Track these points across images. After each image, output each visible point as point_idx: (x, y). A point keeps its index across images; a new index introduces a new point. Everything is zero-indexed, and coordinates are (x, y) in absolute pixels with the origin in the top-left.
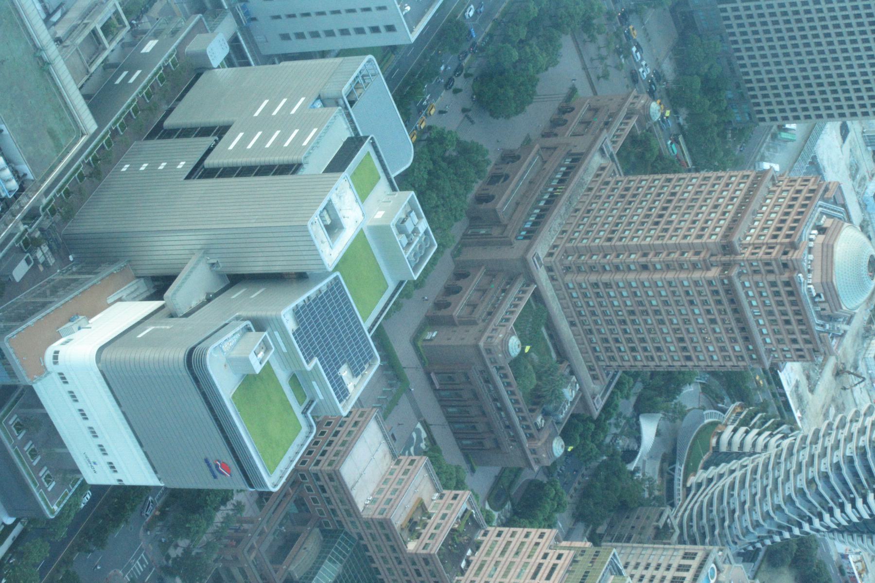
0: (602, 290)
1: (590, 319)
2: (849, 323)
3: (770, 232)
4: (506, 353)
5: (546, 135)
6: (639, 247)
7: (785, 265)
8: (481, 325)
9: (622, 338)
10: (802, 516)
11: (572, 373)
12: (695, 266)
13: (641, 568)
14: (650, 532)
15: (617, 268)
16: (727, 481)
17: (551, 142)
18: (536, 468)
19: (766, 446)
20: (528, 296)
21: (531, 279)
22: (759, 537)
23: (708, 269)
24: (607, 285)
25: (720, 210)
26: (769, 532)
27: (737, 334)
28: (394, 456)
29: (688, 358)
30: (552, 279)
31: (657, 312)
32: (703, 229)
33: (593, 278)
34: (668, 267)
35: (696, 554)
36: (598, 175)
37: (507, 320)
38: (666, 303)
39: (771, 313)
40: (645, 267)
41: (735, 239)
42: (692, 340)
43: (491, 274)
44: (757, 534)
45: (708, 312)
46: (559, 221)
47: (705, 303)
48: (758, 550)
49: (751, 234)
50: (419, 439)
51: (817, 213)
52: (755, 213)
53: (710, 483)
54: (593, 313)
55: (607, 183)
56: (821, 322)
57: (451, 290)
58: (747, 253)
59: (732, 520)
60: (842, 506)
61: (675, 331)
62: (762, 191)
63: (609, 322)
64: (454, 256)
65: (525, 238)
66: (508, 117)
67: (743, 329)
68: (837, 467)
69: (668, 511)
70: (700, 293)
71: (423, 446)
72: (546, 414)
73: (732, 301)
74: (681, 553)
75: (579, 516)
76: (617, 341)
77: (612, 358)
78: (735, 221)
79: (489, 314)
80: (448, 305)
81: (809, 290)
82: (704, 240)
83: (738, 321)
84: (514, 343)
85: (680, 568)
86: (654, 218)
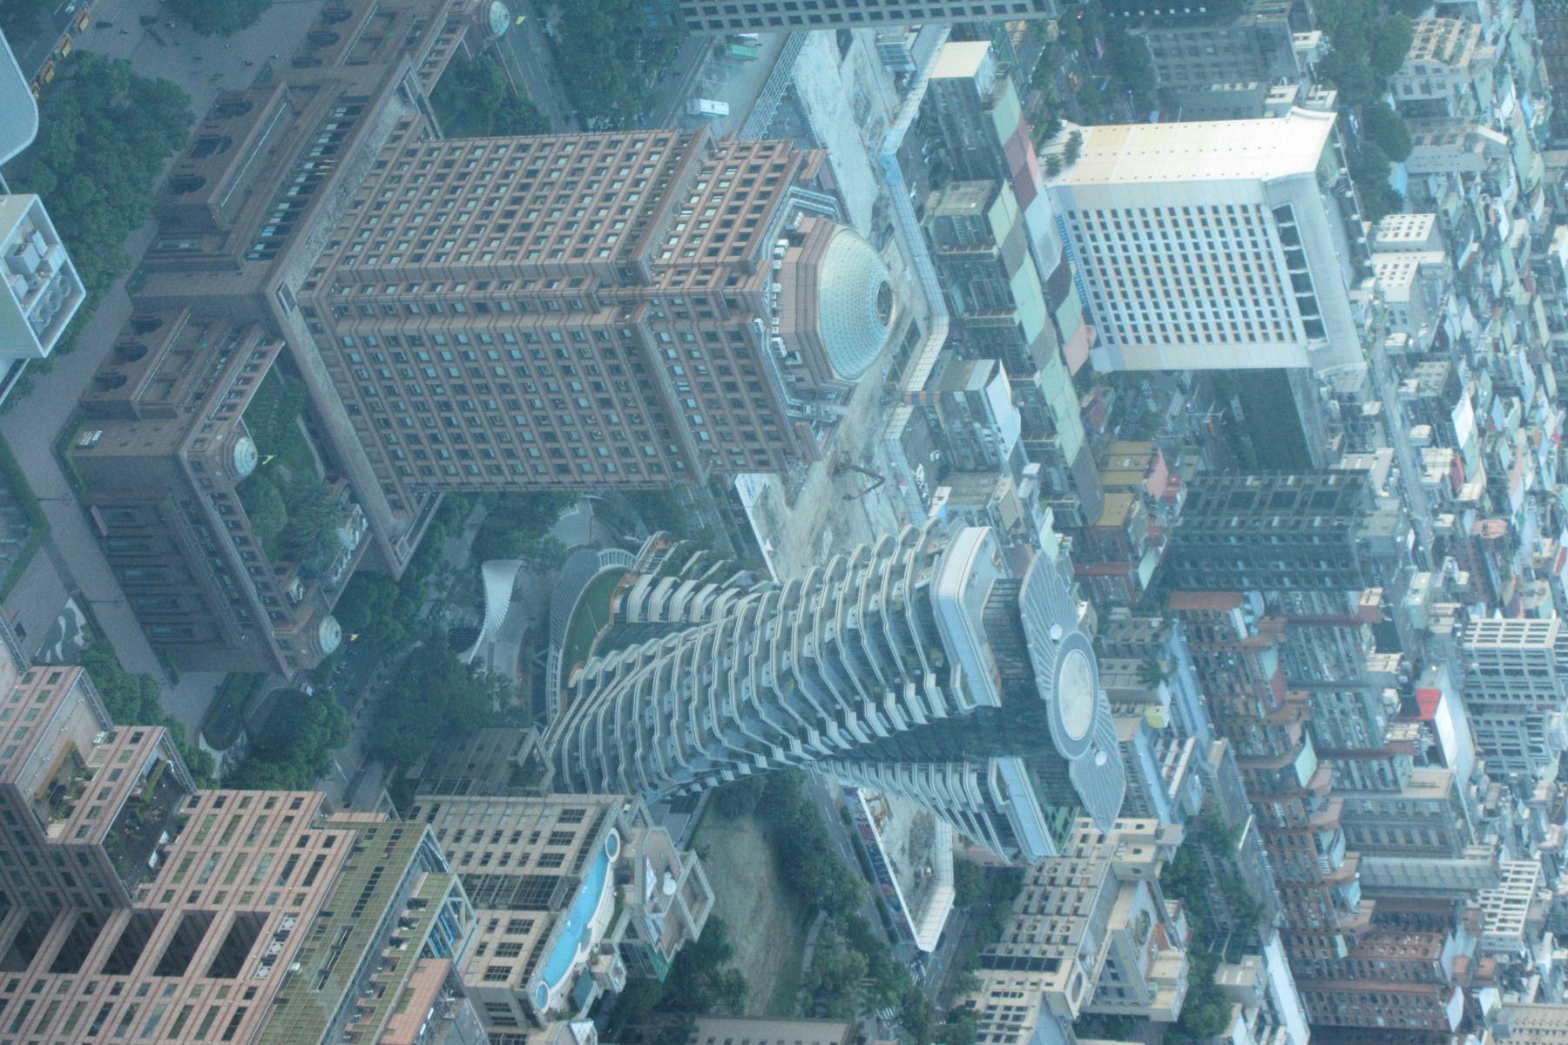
0: (405, 349)
1: (385, 401)
2: (846, 401)
3: (703, 244)
4: (230, 468)
5: (297, 63)
6: (471, 272)
7: (732, 303)
8: (184, 417)
9: (444, 435)
10: (770, 735)
11: (354, 499)
12: (571, 306)
13: (485, 840)
14: (503, 773)
15: (432, 310)
16: (639, 677)
17: (306, 76)
18: (290, 674)
19: (709, 611)
20: (269, 363)
21: (274, 332)
22: (696, 774)
23: (596, 312)
24: (414, 341)
25: (616, 204)
26: (714, 764)
27: (649, 426)
28: (20, 667)
29: (564, 469)
30: (315, 329)
31: (504, 388)
32: (585, 239)
33: (389, 327)
34: (524, 307)
35: (582, 812)
36: (395, 138)
37: (232, 408)
38: (521, 372)
39: (707, 387)
40: (482, 308)
41: (642, 258)
42: (568, 436)
43: (203, 321)
44: (692, 769)
45: (597, 387)
46: (325, 223)
47: (590, 371)
48: (696, 795)
49: (673, 248)
50: (72, 629)
51: (788, 207)
52: (677, 209)
53: (608, 679)
54: (390, 391)
55: (413, 153)
56: (797, 402)
57: (128, 353)
58: (664, 283)
59: (649, 747)
60: (840, 718)
61: (539, 421)
62: (691, 168)
63: (420, 407)
64: (131, 290)
65: (263, 256)
66: (227, 32)
67: (658, 417)
68: (831, 649)
69: (533, 735)
70: (581, 353)
71: (79, 639)
72: (307, 577)
73: (638, 368)
74: (557, 811)
75: (371, 753)
76: (434, 439)
77: (427, 471)
78: (642, 224)
79: (198, 396)
80: (121, 381)
81: (775, 346)
82: (588, 258)
83: (650, 401)
84: (245, 452)
85: (556, 838)
86: (497, 219)
